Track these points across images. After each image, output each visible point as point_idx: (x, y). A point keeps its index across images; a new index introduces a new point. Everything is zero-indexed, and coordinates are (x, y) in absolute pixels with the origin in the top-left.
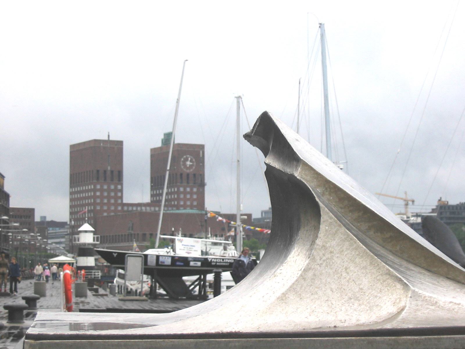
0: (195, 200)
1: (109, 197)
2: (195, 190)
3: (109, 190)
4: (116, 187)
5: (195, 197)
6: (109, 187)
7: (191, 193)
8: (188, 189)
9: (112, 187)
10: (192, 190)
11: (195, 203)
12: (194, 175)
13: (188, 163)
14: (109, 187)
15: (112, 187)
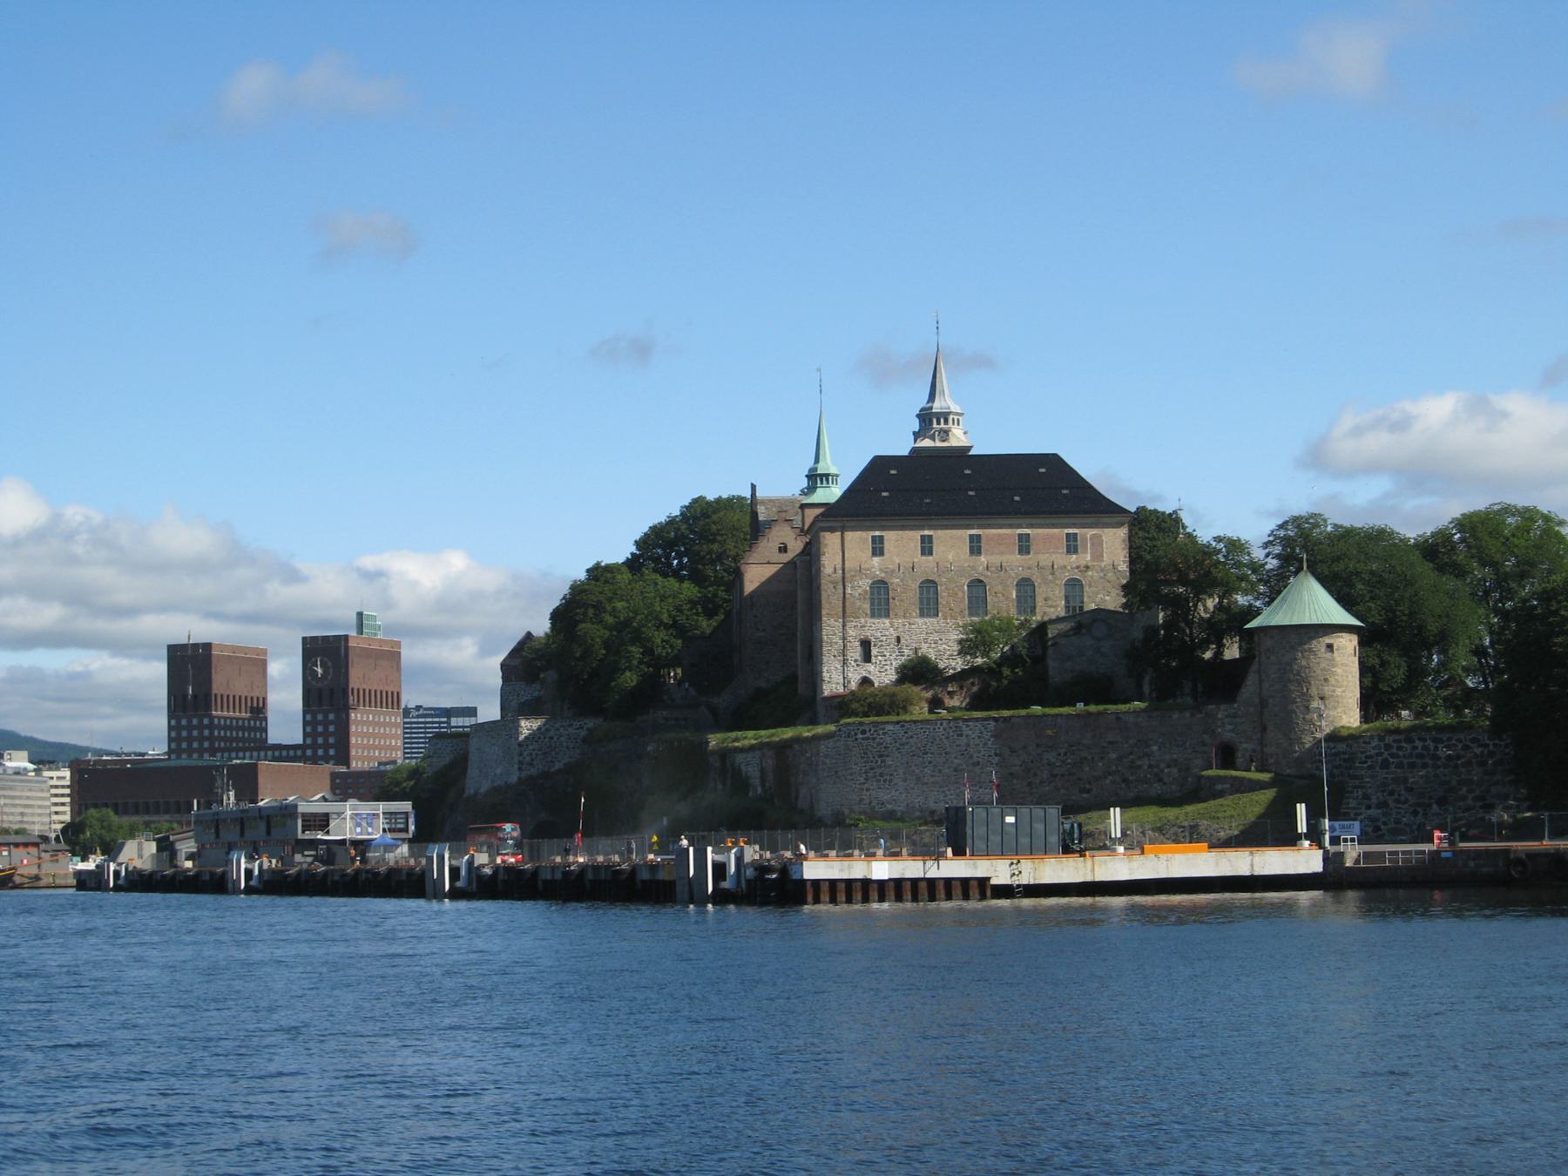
0: (332, 734)
1: (190, 739)
2: (331, 717)
3: (190, 727)
4: (201, 722)
5: (332, 728)
6: (190, 722)
7: (326, 723)
8: (320, 717)
9: (195, 722)
10: (326, 717)
11: (331, 740)
12: (332, 691)
13: (319, 670)
14: (190, 722)
15: (195, 722)
